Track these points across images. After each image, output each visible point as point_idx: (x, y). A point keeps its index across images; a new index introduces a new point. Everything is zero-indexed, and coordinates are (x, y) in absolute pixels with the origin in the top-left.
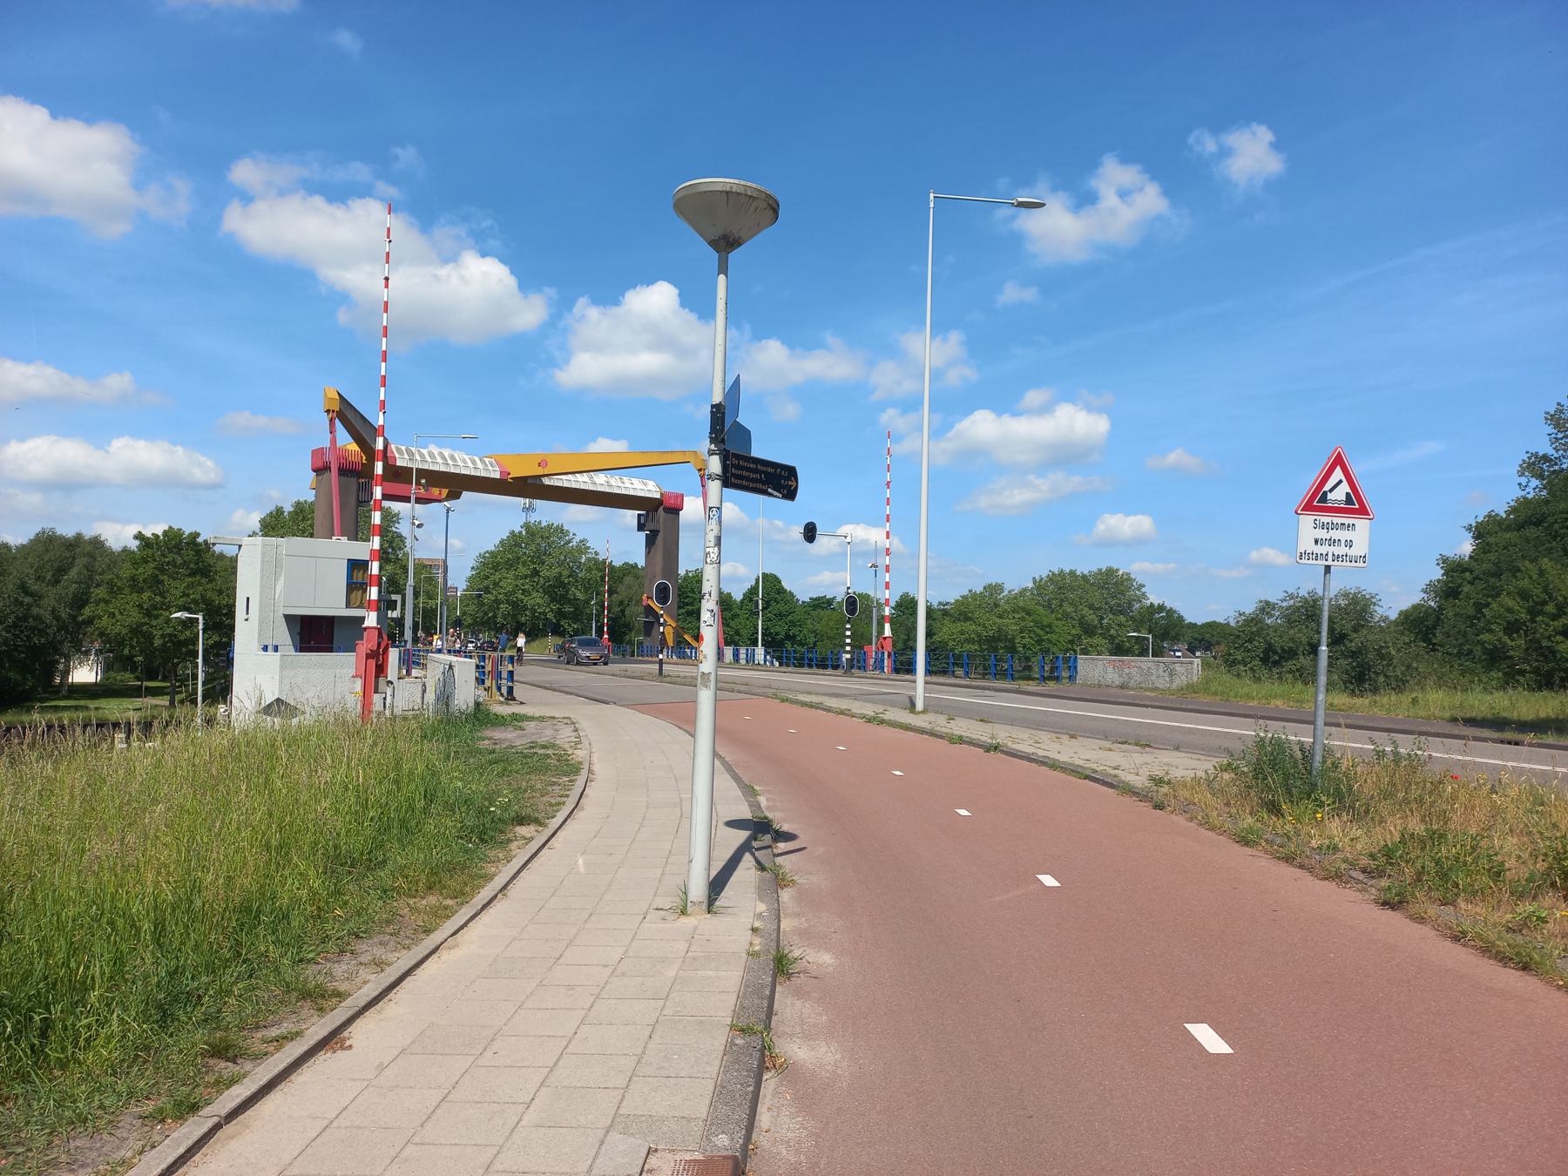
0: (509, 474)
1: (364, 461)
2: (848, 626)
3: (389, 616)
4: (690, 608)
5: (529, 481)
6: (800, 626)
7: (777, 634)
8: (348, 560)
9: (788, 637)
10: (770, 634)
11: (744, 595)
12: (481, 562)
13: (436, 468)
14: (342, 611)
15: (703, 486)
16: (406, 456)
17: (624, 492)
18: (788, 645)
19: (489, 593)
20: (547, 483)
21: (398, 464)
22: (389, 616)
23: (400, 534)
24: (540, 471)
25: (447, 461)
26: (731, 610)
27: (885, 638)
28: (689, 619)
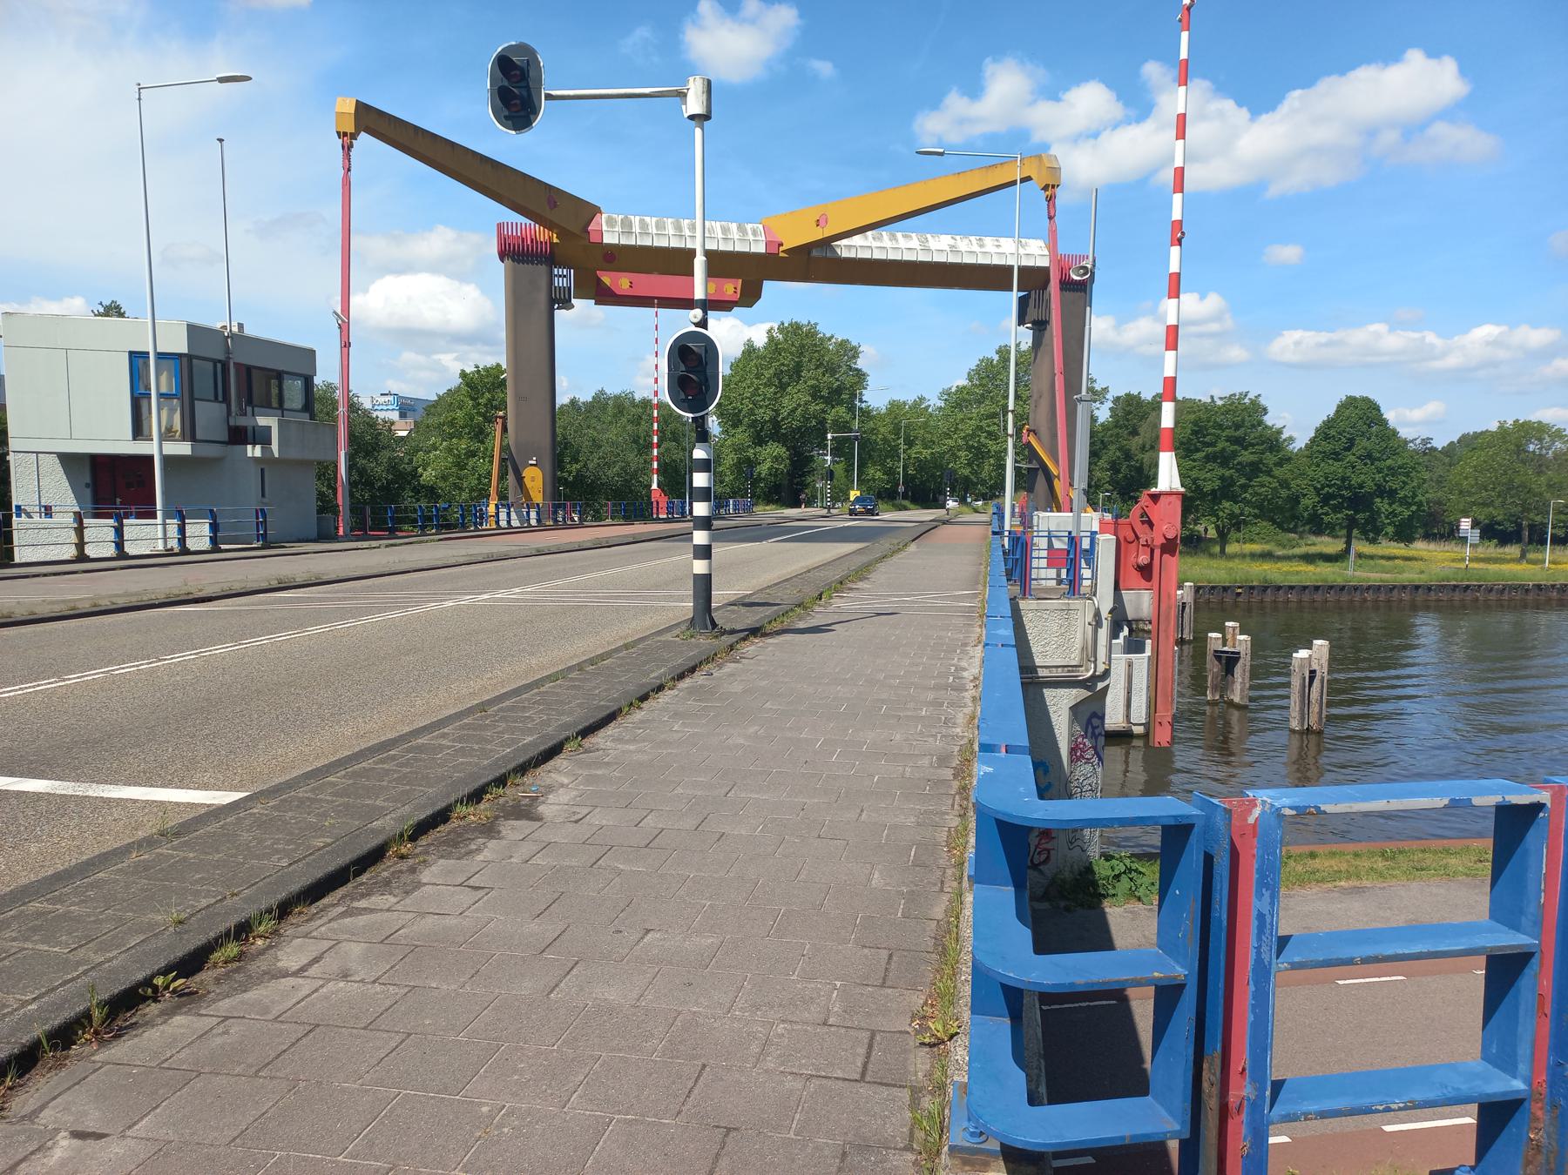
0: (781, 245)
1: (555, 240)
2: (699, 453)
3: (250, 454)
4: (1210, 449)
5: (815, 253)
6: (1407, 475)
7: (1361, 486)
8: (131, 353)
9: (1381, 491)
10: (1349, 488)
11: (1317, 430)
12: (946, 400)
13: (663, 243)
14: (127, 446)
15: (1050, 218)
16: (618, 228)
17: (982, 260)
18: (1382, 505)
19: (951, 438)
20: (845, 254)
21: (605, 241)
22: (250, 454)
23: (860, 370)
24: (818, 234)
25: (681, 231)
26: (1278, 451)
27: (1155, 498)
28: (1209, 466)
